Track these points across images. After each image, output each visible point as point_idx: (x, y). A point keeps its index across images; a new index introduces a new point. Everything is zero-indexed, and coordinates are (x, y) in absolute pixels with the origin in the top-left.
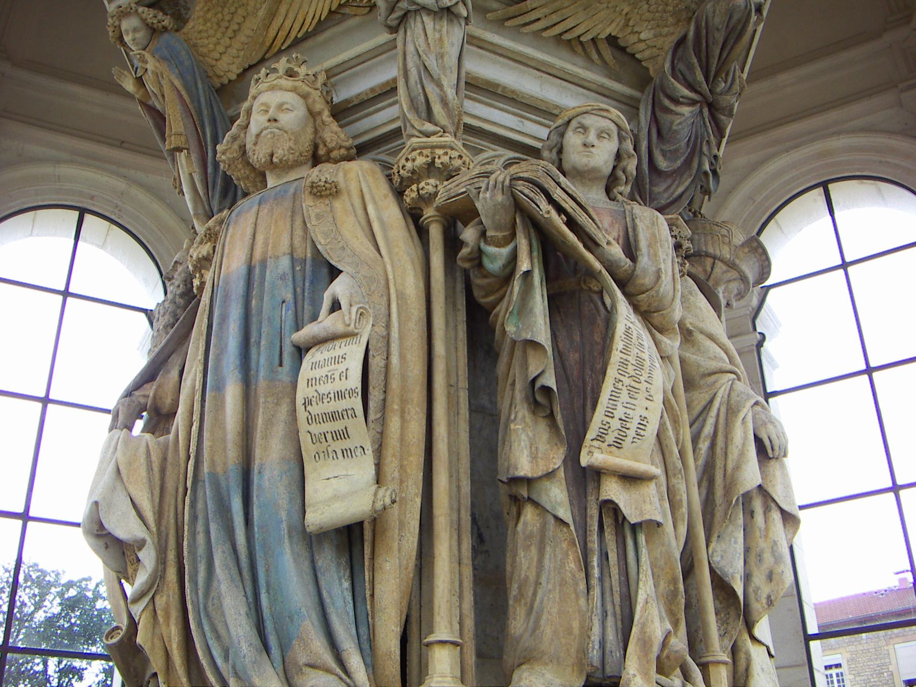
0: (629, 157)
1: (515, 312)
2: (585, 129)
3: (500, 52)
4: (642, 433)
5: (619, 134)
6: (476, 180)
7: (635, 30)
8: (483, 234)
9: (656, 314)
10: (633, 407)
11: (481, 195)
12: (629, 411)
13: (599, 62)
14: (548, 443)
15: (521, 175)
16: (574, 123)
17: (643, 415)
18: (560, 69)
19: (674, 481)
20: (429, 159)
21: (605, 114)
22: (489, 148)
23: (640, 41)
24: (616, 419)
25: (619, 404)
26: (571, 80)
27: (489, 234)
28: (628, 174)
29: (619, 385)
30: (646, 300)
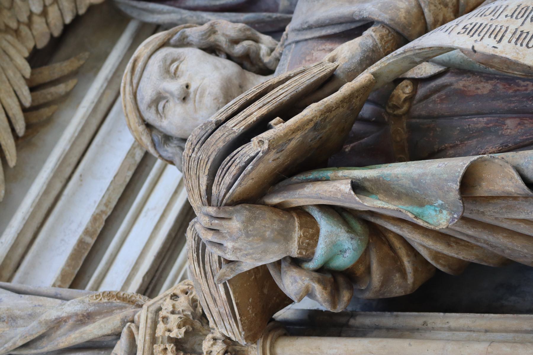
1: (417, 210)
2: (159, 99)
3: (29, 236)
5: (175, 46)
6: (208, 267)
7: (24, 18)
8: (296, 262)
11: (230, 257)
13: (71, 83)
15: (203, 188)
16: (150, 116)
18: (73, 144)
20: (171, 347)
21: (140, 64)
22: (181, 268)
23: (44, 13)
27: (295, 252)
28: (241, 35)
30: (433, 7)
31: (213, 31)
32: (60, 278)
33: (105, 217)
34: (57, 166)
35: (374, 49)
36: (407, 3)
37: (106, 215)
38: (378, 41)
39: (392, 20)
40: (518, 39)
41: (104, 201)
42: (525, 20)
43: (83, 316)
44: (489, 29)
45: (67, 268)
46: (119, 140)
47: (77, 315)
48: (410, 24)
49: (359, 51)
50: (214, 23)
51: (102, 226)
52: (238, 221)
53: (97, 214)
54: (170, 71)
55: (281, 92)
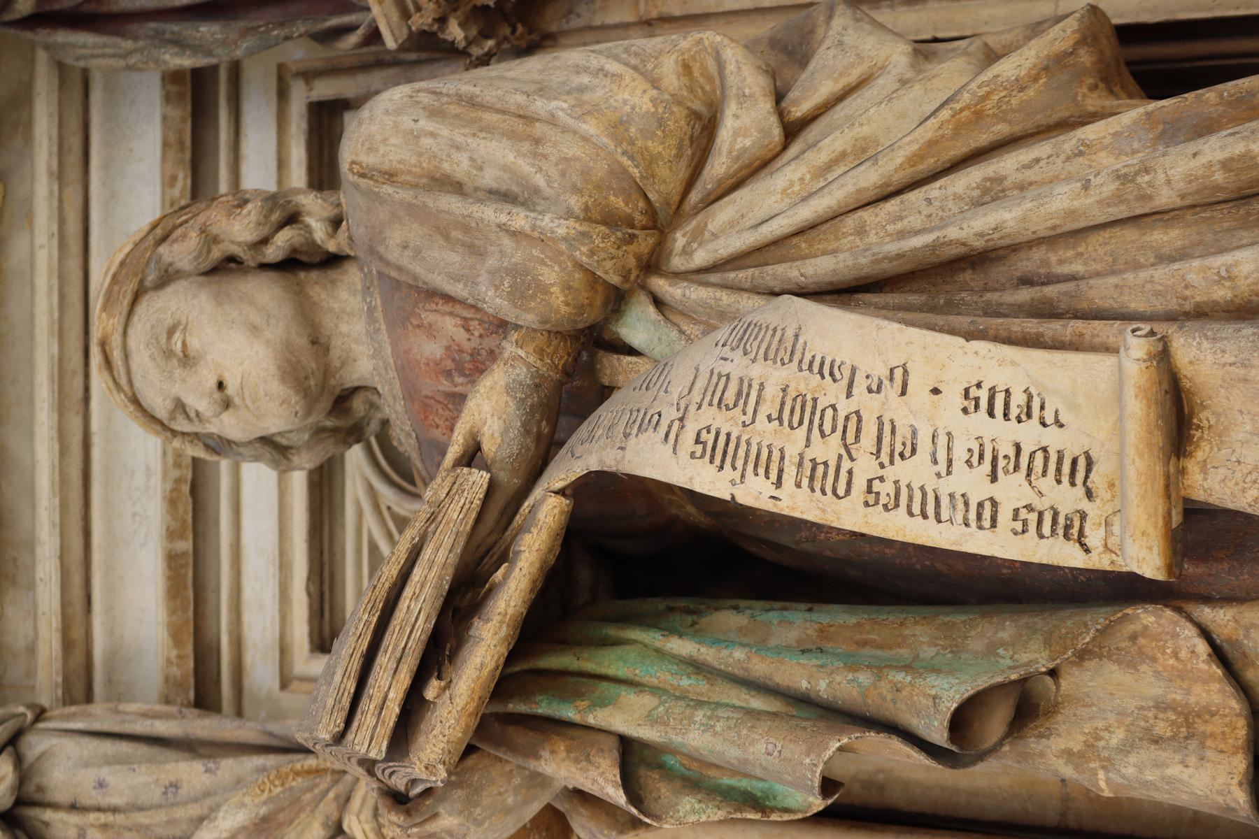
0: (216, 240)
4: (1018, 399)
9: (652, 196)
10: (942, 441)
12: (960, 454)
14: (1132, 665)
16: (181, 425)
17: (960, 402)
19: (1166, 197)
24: (996, 491)
25: (946, 487)
29: (886, 489)
31: (211, 239)
32: (171, 643)
33: (186, 488)
34: (56, 395)
35: (537, 381)
36: (556, 268)
37: (186, 481)
38: (539, 364)
39: (544, 322)
40: (812, 478)
41: (170, 459)
42: (810, 430)
43: (256, 824)
44: (748, 451)
45: (174, 618)
47: (244, 828)
48: (581, 308)
49: (512, 405)
50: (205, 223)
51: (190, 507)
52: (450, 815)
53: (172, 491)
55: (415, 608)
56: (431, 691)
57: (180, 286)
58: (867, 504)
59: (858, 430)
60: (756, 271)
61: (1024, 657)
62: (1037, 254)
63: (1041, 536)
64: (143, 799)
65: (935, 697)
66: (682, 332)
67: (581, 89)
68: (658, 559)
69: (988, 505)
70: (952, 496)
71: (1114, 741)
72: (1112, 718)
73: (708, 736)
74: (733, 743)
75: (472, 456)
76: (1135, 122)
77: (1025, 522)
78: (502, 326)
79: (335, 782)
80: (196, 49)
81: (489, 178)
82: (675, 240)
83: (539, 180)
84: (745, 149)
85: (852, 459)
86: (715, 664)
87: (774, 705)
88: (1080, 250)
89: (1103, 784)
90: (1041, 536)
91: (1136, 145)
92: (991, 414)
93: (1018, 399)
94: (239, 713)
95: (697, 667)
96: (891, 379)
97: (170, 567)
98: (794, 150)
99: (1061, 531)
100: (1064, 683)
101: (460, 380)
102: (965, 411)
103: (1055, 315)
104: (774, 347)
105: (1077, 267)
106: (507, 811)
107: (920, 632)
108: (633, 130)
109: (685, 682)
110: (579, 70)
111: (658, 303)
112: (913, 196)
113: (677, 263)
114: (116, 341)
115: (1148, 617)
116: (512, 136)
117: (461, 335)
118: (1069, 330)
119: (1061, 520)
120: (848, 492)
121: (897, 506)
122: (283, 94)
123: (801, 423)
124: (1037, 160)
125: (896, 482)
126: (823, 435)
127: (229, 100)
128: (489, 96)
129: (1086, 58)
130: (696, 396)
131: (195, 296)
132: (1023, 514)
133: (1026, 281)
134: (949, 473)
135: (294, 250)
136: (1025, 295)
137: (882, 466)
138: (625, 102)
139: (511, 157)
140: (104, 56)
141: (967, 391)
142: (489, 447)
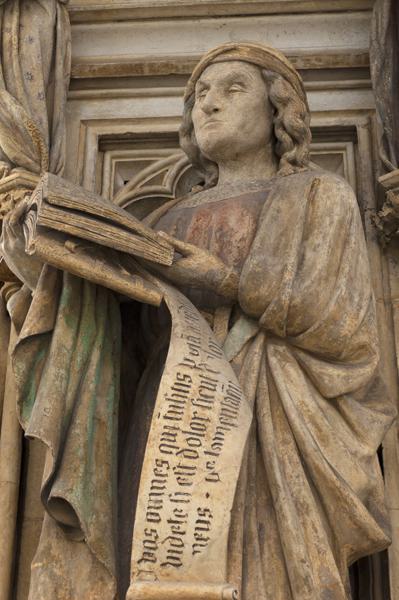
0: (285, 105)
3: (147, 15)
4: (205, 534)
5: (264, 78)
9: (301, 336)
10: (186, 498)
12: (180, 506)
14: (89, 579)
16: (198, 88)
17: (203, 507)
24: (164, 522)
25: (165, 498)
26: (271, 10)
28: (289, 129)
29: (163, 470)
31: (285, 102)
33: (173, 71)
39: (241, 288)
41: (186, 64)
42: (190, 433)
44: (180, 402)
46: (278, 36)
47: (12, 117)
49: (204, 273)
54: (230, 86)
55: (108, 235)
56: (70, 244)
57: (263, 88)
58: (157, 460)
59: (190, 457)
60: (266, 391)
61: (92, 529)
62: (273, 534)
63: (144, 542)
64: (25, 63)
65: (72, 490)
66: (239, 353)
67: (351, 299)
68: (136, 342)
69: (157, 518)
70: (161, 501)
71: (55, 570)
72: (65, 568)
73: (53, 377)
74: (51, 390)
75: (183, 254)
76: (334, 578)
77: (150, 535)
78: (240, 264)
79: (36, 162)
80: (380, 77)
81: (309, 255)
82: (281, 345)
83: (308, 283)
84: (323, 380)
85: (177, 454)
86: (88, 374)
87: (69, 405)
88: (275, 555)
89: (36, 565)
90: (144, 542)
91: (324, 578)
92: (198, 521)
93: (205, 534)
94: (69, 99)
95: (86, 364)
96: (213, 474)
97: (136, 65)
98: (323, 403)
99: (146, 551)
100: (81, 546)
101: (218, 235)
102: (199, 509)
103: (244, 545)
104: (228, 413)
105: (266, 555)
106: (19, 268)
107: (101, 474)
108: (332, 327)
109: (79, 359)
110: (361, 295)
111: (252, 340)
112: (301, 468)
113: (271, 348)
114: (236, 55)
115: (111, 586)
116: (329, 265)
117: (238, 236)
118: (237, 554)
119: (152, 551)
120: (162, 451)
121: (157, 475)
122: (361, 112)
123: (193, 429)
124: (316, 531)
125: (167, 475)
126: (188, 440)
127: (359, 84)
128: (348, 251)
129: (366, 544)
130: (206, 374)
131: (258, 96)
132: (154, 534)
133: (261, 528)
134: (172, 500)
135: (281, 143)
136: (254, 528)
137: (174, 468)
138: (345, 322)
139: (319, 267)
140: (377, 28)
141: (208, 510)
142: (184, 263)
